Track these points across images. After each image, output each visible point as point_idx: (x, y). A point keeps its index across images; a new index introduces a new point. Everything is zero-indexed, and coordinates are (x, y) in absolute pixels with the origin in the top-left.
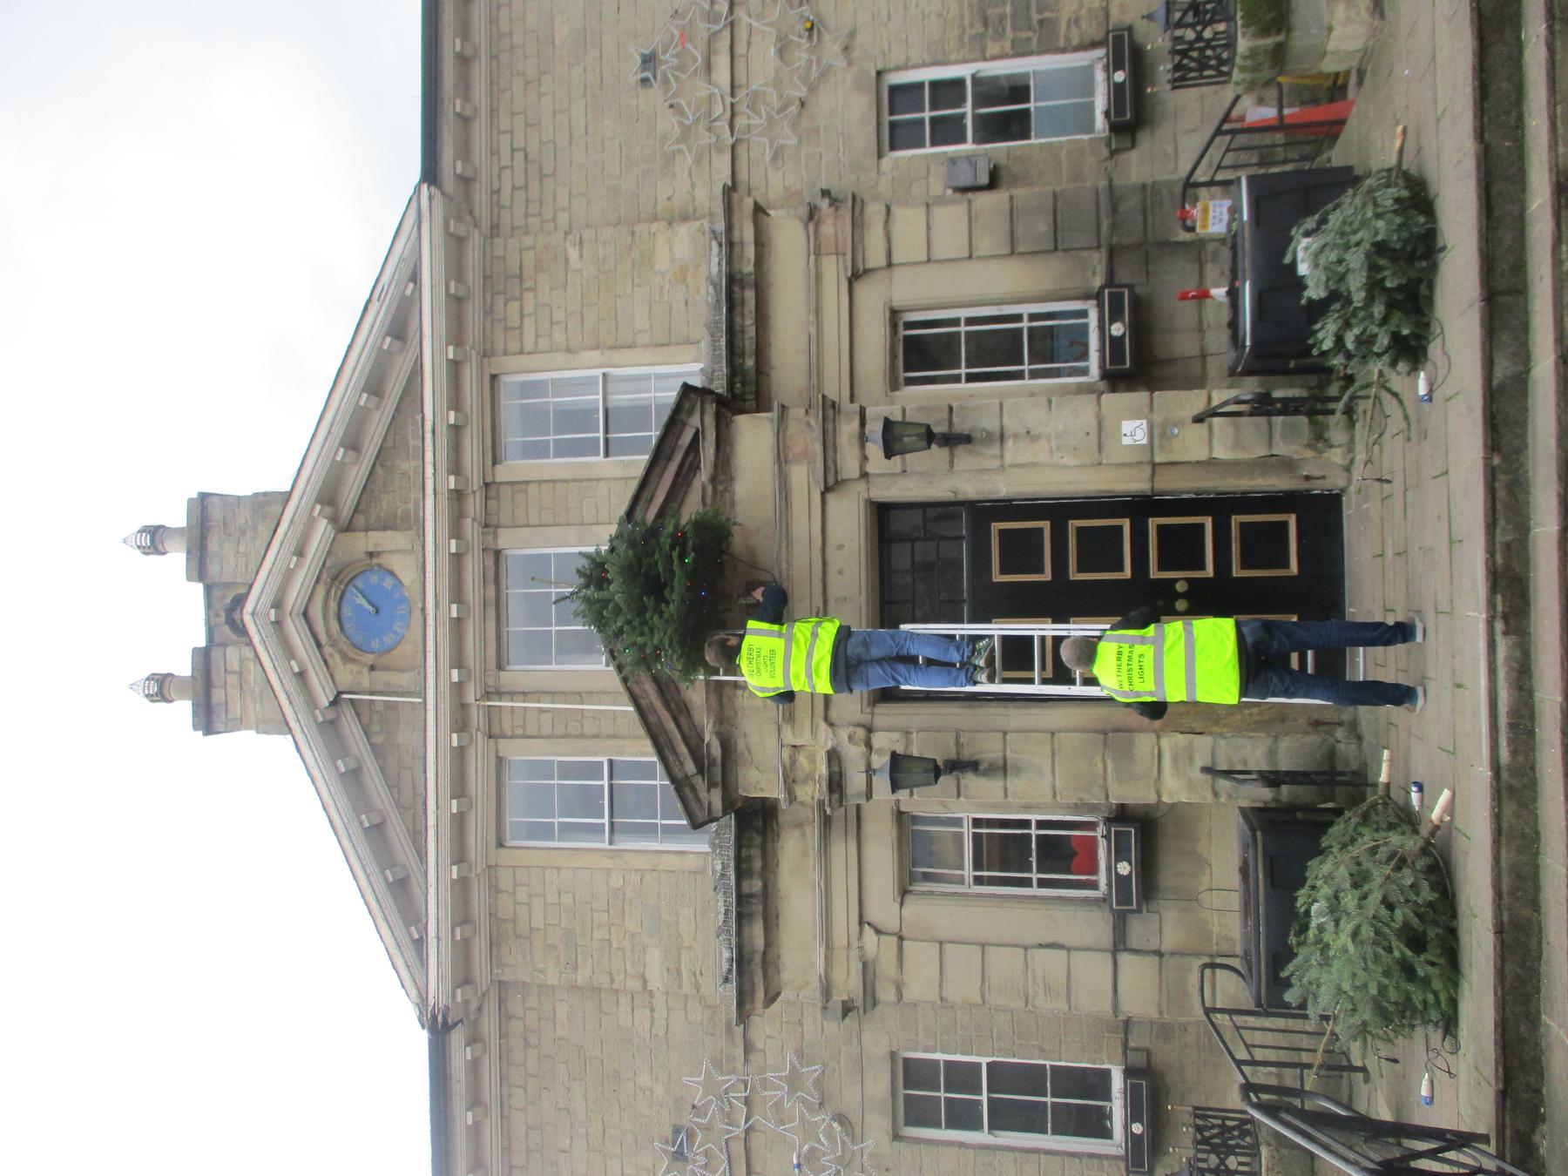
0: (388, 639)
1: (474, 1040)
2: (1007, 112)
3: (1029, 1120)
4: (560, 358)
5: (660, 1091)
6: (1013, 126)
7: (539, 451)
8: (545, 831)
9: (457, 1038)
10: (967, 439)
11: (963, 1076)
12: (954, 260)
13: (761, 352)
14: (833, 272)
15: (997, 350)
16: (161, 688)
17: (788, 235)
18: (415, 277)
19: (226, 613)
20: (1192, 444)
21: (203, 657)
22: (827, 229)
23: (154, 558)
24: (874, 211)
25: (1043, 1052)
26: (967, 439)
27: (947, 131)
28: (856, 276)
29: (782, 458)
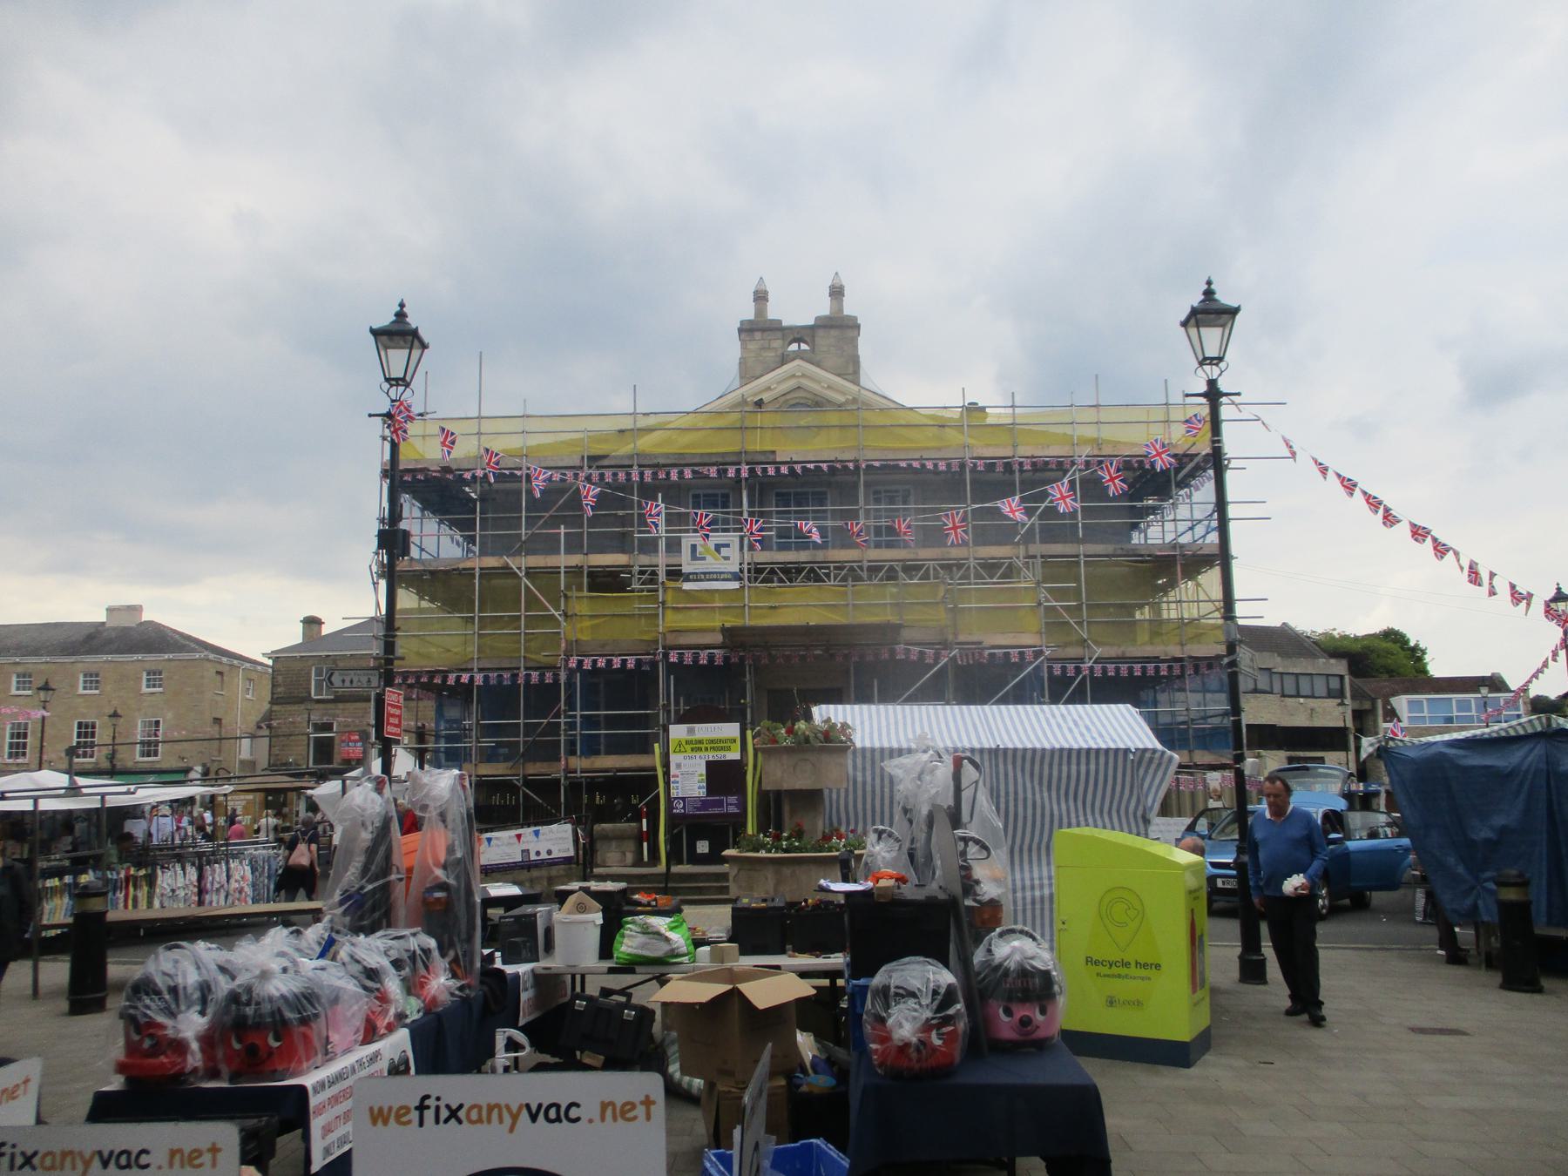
16: (761, 297)
19: (799, 334)
21: (775, 328)
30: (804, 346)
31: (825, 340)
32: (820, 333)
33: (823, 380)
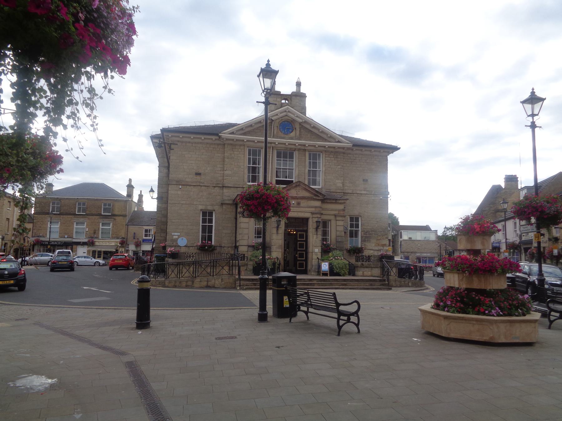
0: (281, 130)
1: (216, 139)
2: (353, 234)
3: (204, 231)
4: (324, 164)
5: (206, 171)
6: (351, 236)
7: (310, 159)
8: (249, 155)
9: (217, 137)
10: (317, 230)
11: (211, 221)
12: (337, 229)
13: (327, 203)
14: (337, 212)
15: (325, 233)
17: (341, 207)
18: (339, 142)
19: (286, 97)
20: (315, 257)
21: (278, 94)
22: (342, 212)
23: (295, 84)
24: (344, 219)
25: (215, 234)
26: (317, 230)
27: (352, 226)
28: (335, 216)
29: (316, 207)
30: (287, 102)
31: (295, 101)
32: (294, 97)
33: (294, 113)
